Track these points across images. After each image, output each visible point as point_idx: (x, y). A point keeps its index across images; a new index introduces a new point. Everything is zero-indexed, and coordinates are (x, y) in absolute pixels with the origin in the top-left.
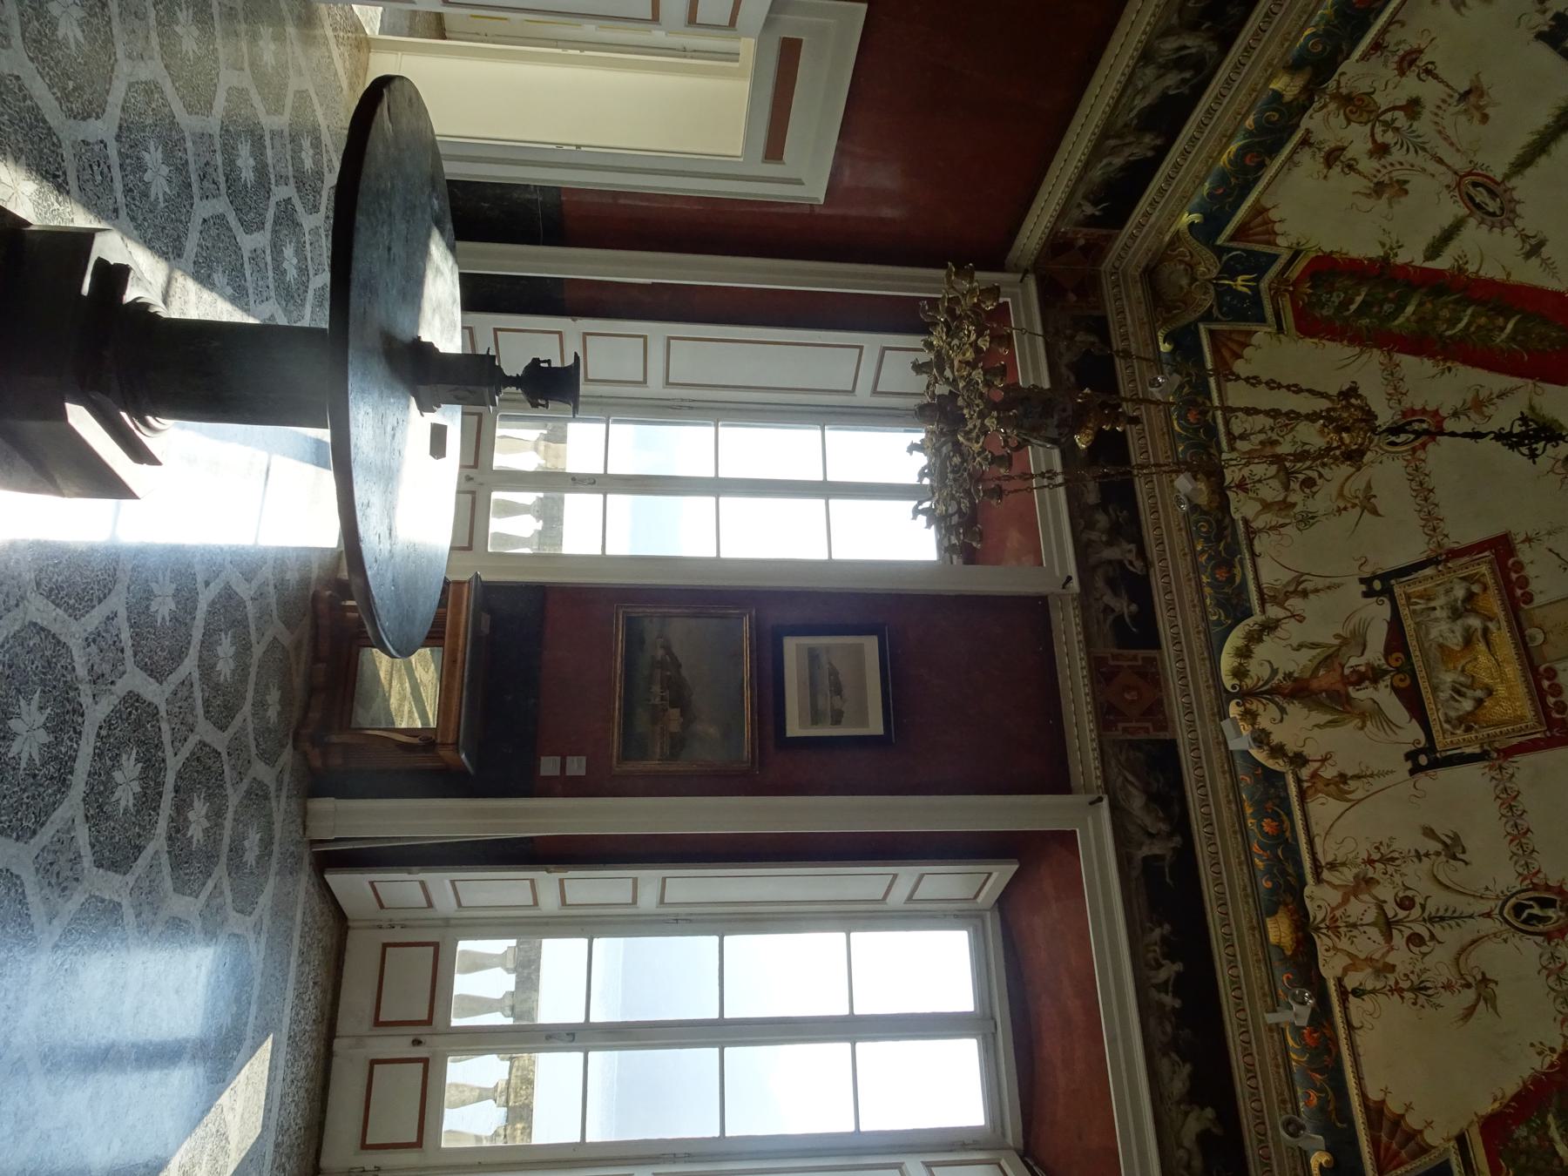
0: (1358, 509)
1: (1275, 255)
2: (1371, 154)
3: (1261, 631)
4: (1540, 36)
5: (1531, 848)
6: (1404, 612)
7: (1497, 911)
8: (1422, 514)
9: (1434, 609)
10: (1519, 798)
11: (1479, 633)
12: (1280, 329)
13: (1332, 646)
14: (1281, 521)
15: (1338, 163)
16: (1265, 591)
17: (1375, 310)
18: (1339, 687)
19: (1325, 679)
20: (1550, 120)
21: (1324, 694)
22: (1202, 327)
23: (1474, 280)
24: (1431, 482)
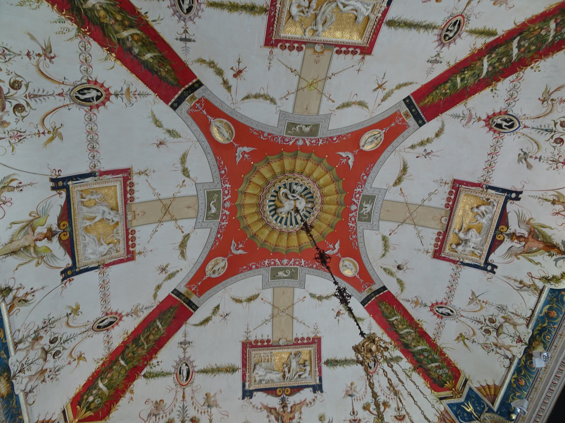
0: (479, 298)
1: (449, 406)
2: (389, 406)
3: (551, 280)
4: (322, 392)
5: (492, 148)
6: (485, 253)
7: (520, 128)
8: (457, 282)
9: (473, 248)
11: (462, 231)
12: (466, 381)
13: (524, 257)
14: (512, 315)
15: (401, 414)
16: (538, 294)
17: (430, 357)
18: (531, 239)
19: (534, 245)
20: (338, 367)
21: (540, 240)
22: (495, 408)
23: (394, 341)
24: (448, 290)
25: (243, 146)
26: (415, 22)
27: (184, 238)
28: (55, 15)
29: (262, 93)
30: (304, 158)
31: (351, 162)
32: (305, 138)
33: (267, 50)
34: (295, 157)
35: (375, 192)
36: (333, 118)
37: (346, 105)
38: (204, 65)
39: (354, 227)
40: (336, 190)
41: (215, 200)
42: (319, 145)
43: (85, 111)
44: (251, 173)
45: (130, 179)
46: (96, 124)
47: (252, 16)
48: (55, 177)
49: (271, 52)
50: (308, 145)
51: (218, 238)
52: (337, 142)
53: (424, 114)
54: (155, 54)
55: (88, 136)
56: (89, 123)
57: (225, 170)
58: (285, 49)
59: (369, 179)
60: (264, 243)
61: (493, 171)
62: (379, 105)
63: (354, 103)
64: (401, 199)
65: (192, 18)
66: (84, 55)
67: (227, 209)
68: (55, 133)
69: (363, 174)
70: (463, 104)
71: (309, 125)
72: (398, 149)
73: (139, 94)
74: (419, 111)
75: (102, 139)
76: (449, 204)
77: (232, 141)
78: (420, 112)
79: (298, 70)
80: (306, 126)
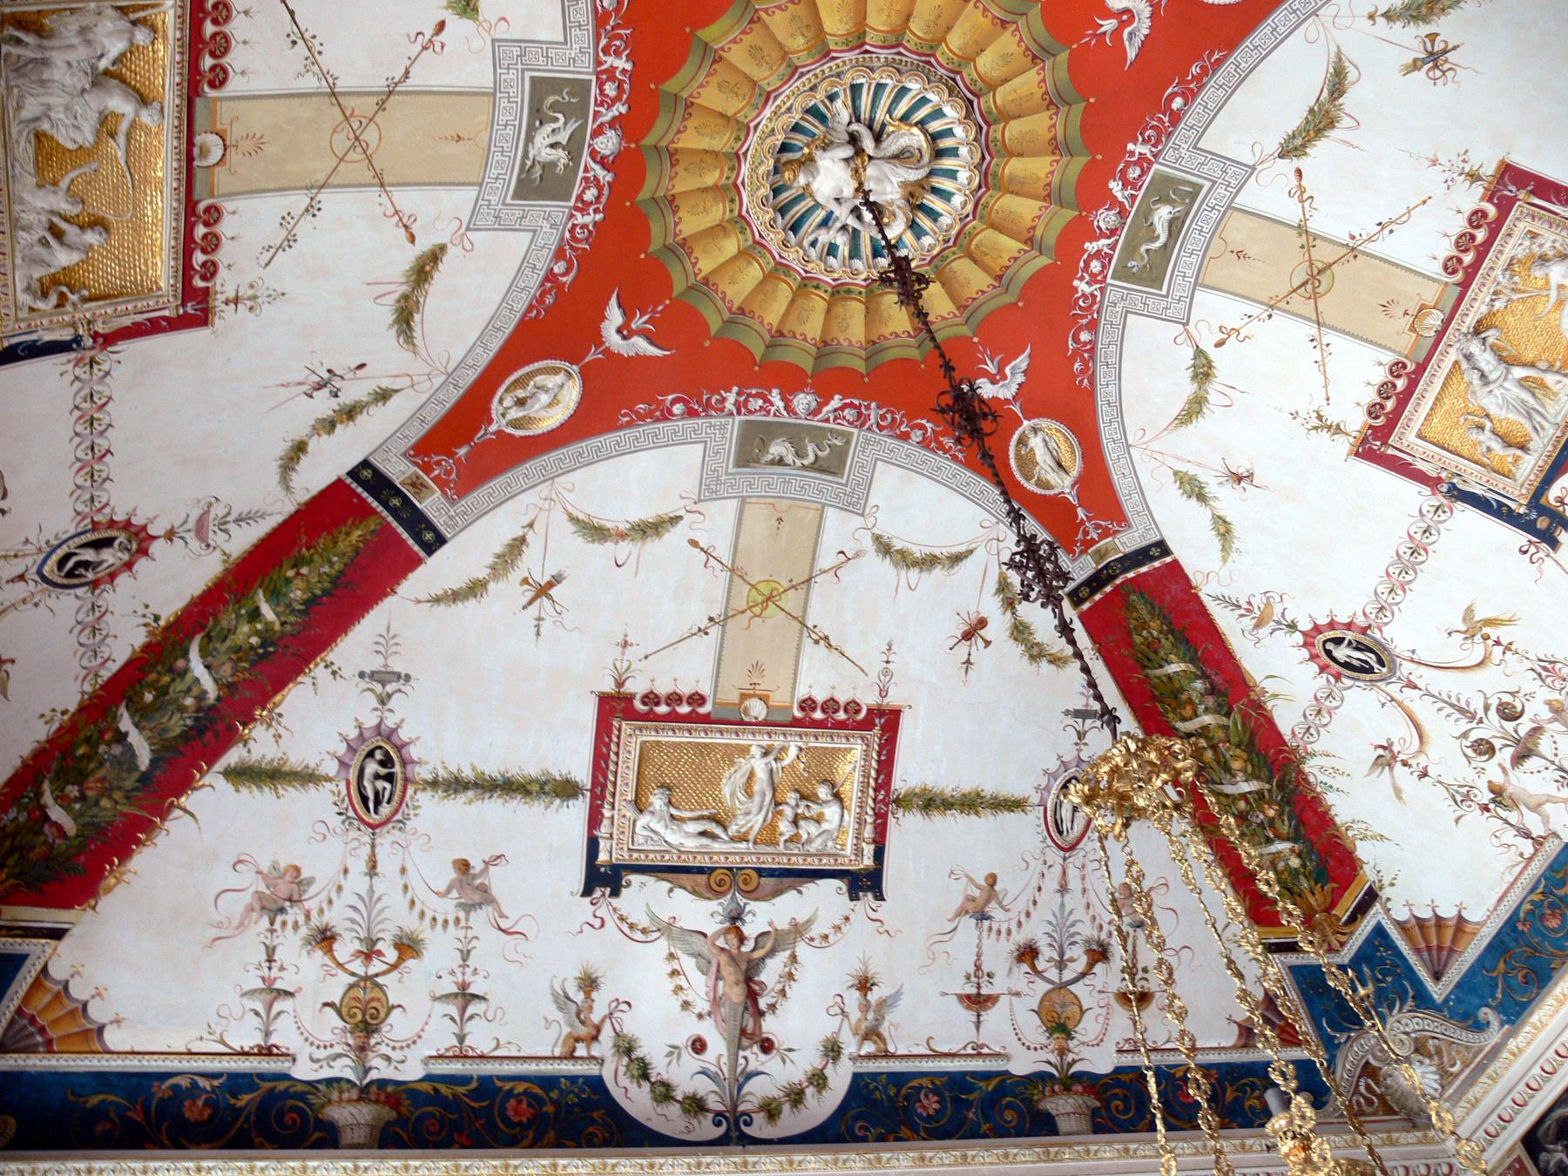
7: (34, 569)
10: (106, 408)
25: (995, 399)
26: (499, 797)
27: (1304, 146)
28: (1330, 798)
29: (914, 574)
30: (791, 341)
31: (614, 316)
32: (786, 419)
33: (893, 700)
34: (825, 347)
35: (518, 213)
36: (690, 485)
37: (648, 530)
38: (1053, 651)
39: (606, 51)
40: (674, 213)
41: (1143, 248)
42: (735, 389)
43: (1381, 631)
44: (986, 309)
45: (1371, 427)
46: (1376, 594)
47: (929, 787)
48: (1544, 546)
49: (883, 693)
50: (775, 392)
51: (1183, 95)
52: (670, 397)
53: (359, 496)
54: (1158, 672)
55: (1410, 582)
56: (1390, 605)
57: (1076, 339)
58: (848, 704)
59: (542, 261)
60: (1009, 18)
61: (77, 407)
62: (531, 525)
63: (622, 536)
64: (407, 199)
65: (1062, 769)
66: (1317, 722)
67: (1114, 203)
68: (1474, 627)
69: (567, 279)
70: (231, 559)
71: (772, 463)
72: (438, 381)
73: (1239, 607)
74: (375, 504)
75: (1384, 558)
76: (206, 224)
77: (1026, 423)
78: (370, 499)
79: (808, 643)
80: (780, 462)
